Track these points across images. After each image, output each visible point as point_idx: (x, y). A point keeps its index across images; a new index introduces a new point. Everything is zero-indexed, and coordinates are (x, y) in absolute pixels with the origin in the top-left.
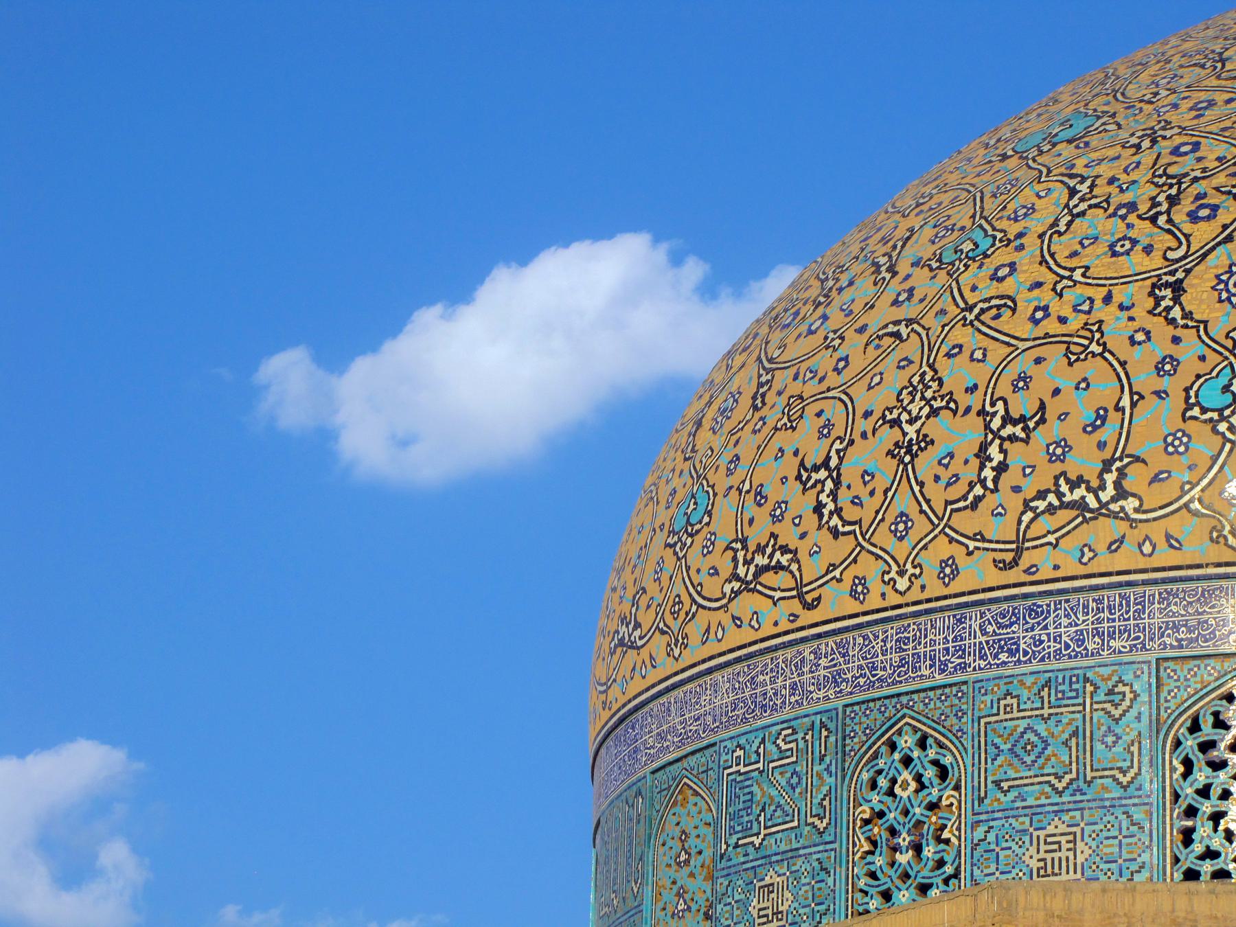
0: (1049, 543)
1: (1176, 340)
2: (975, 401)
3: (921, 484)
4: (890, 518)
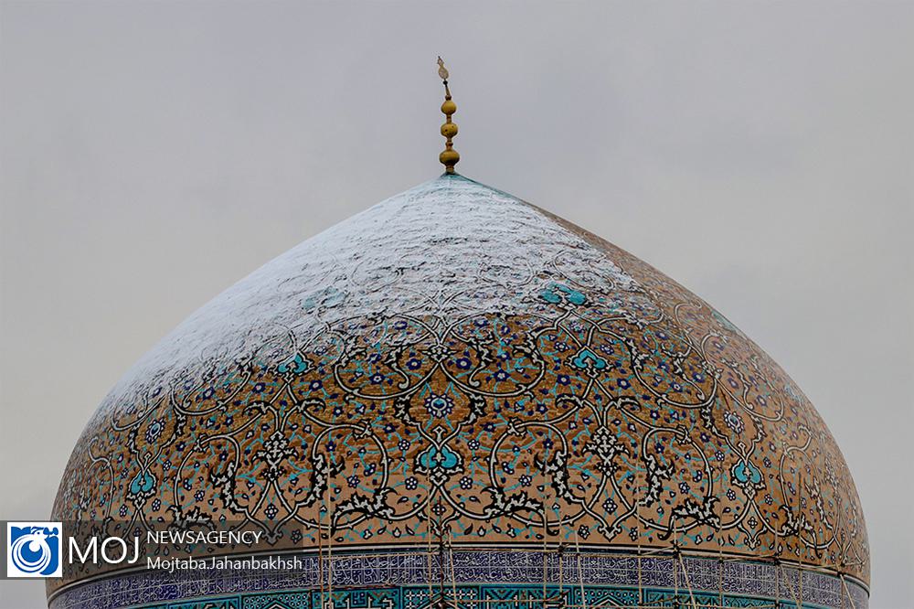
0: (349, 528)
3: (282, 491)
4: (264, 507)
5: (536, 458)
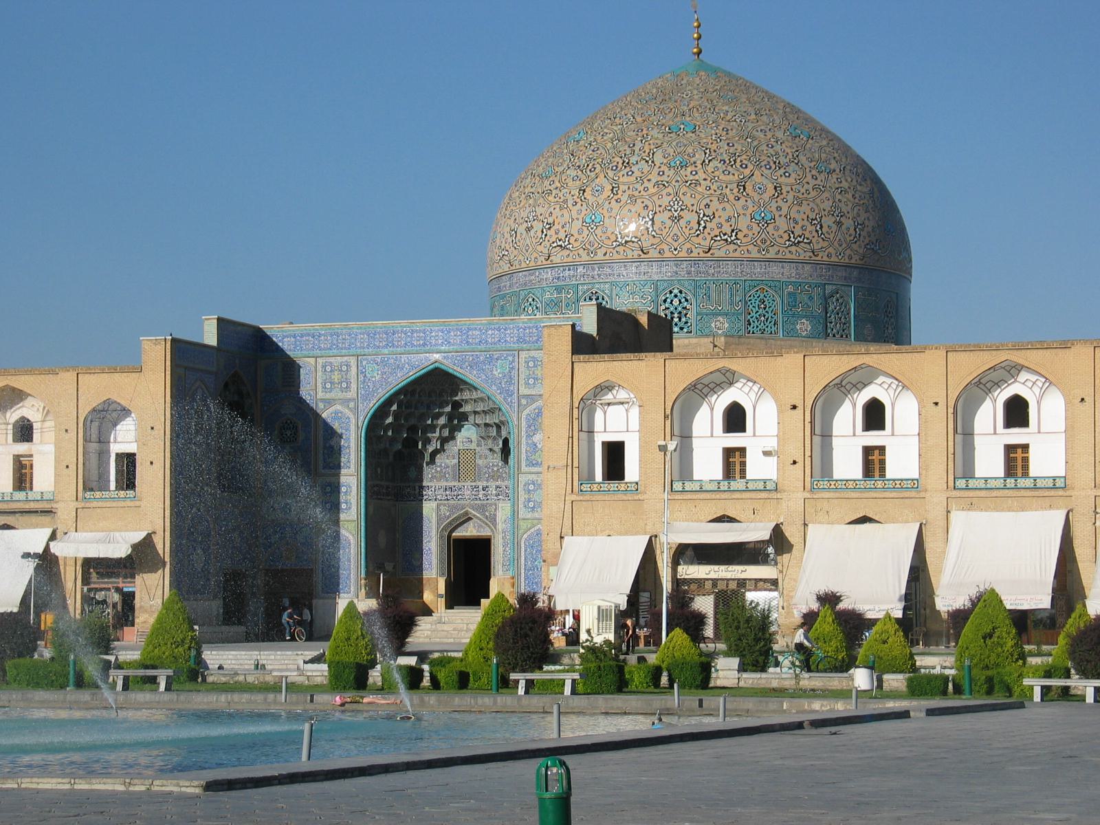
1: (582, 205)
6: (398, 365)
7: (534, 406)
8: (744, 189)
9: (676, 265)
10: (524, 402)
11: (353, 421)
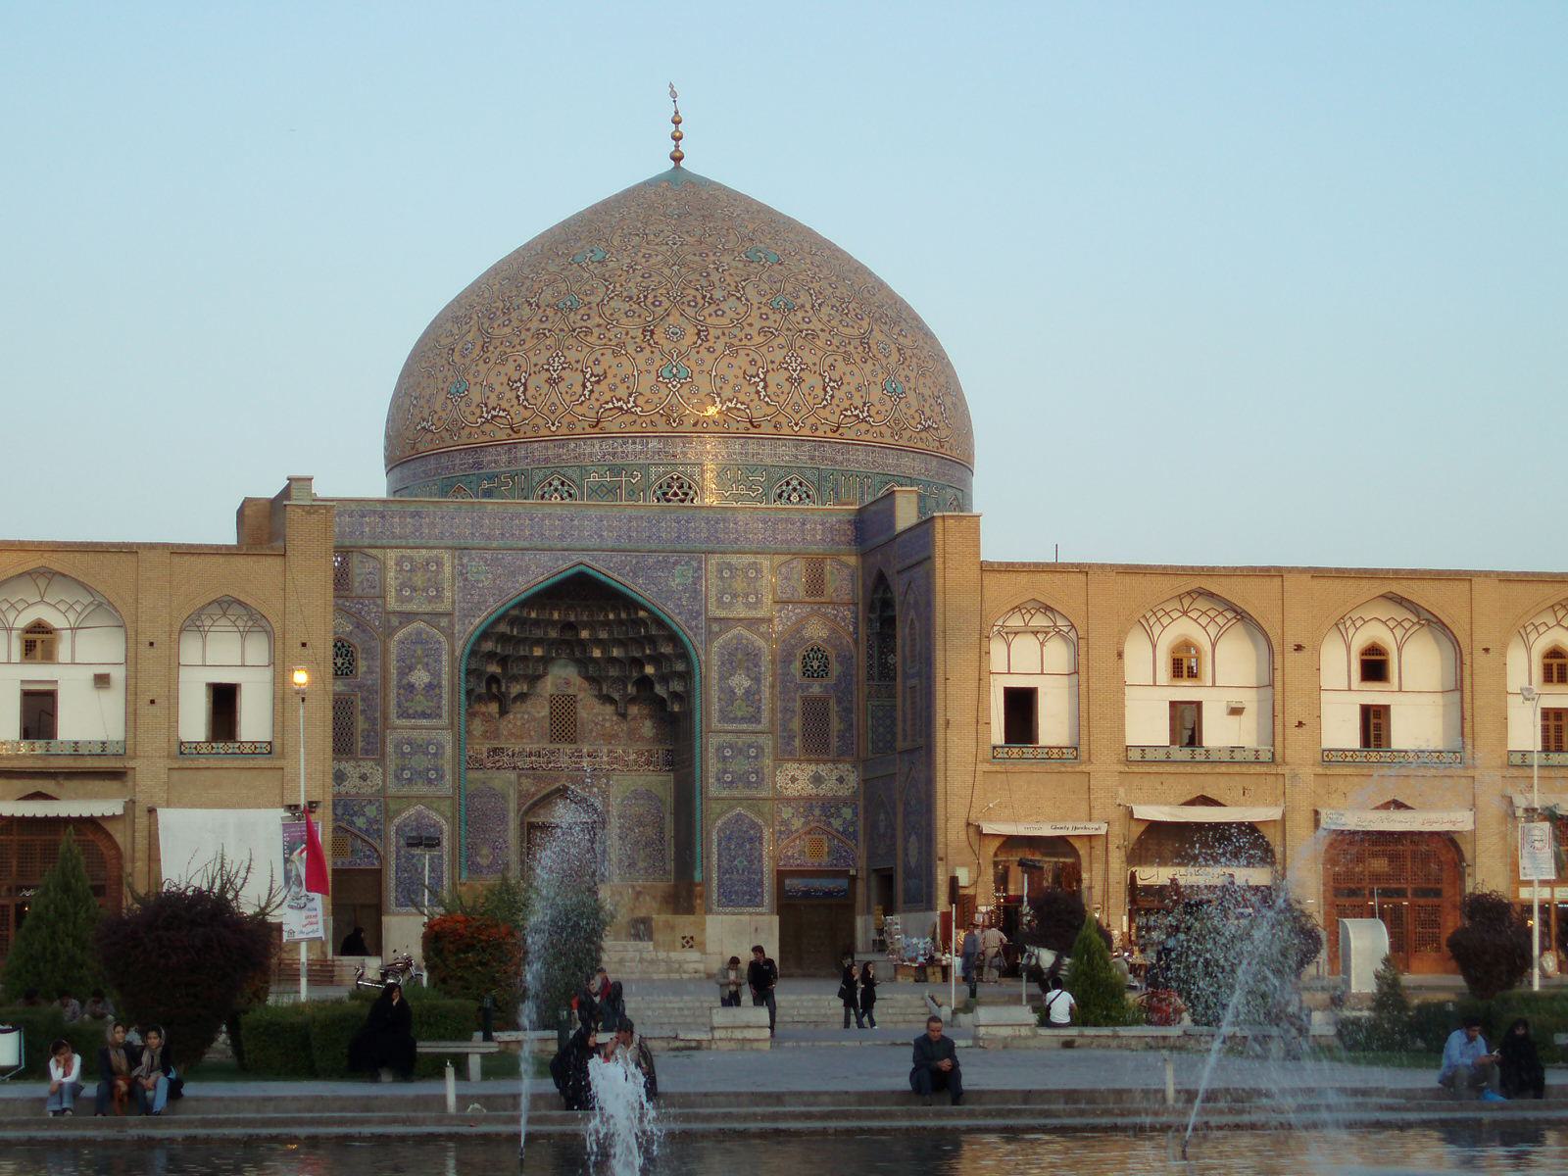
1: (652, 352)
2: (579, 366)
5: (745, 373)
6: (520, 567)
7: (729, 635)
8: (869, 348)
9: (796, 446)
10: (715, 628)
11: (446, 646)
